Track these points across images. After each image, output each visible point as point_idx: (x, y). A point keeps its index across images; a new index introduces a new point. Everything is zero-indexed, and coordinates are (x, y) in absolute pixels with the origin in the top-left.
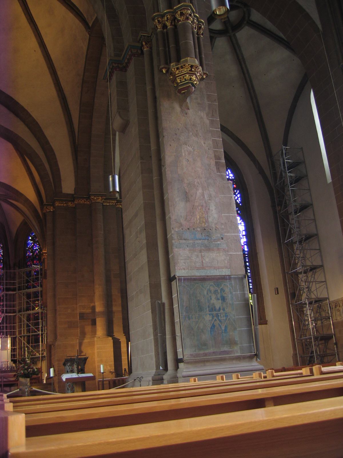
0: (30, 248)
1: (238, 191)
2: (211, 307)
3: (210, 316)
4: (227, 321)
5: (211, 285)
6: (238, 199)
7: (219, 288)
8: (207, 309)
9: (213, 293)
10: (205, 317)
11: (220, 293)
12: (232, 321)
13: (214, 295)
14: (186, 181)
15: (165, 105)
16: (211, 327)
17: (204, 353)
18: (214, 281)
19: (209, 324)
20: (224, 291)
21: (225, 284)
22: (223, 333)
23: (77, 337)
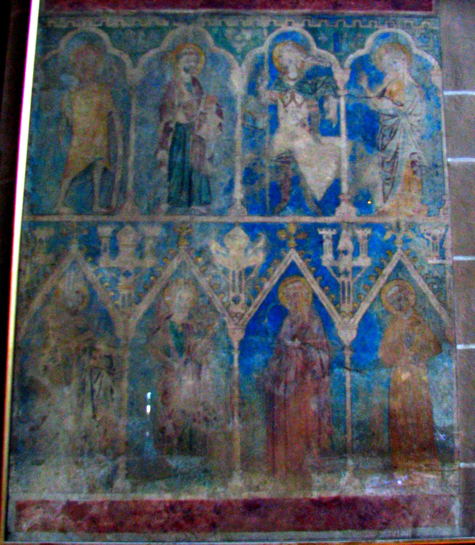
2: (267, 180)
3: (254, 238)
4: (382, 281)
5: (284, 36)
7: (341, 60)
8: (239, 193)
9: (292, 84)
10: (214, 246)
11: (342, 92)
12: (421, 283)
13: (299, 98)
16: (256, 318)
17: (171, 507)
18: (306, 11)
19: (236, 300)
21: (385, 36)
22: (342, 364)
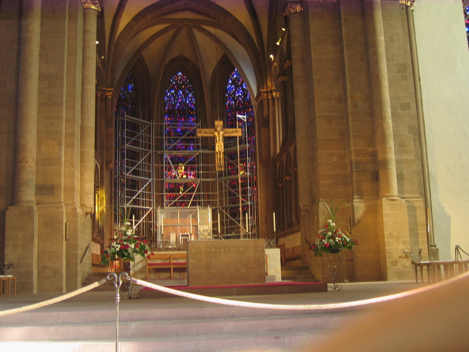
0: (229, 95)
23: (347, 200)
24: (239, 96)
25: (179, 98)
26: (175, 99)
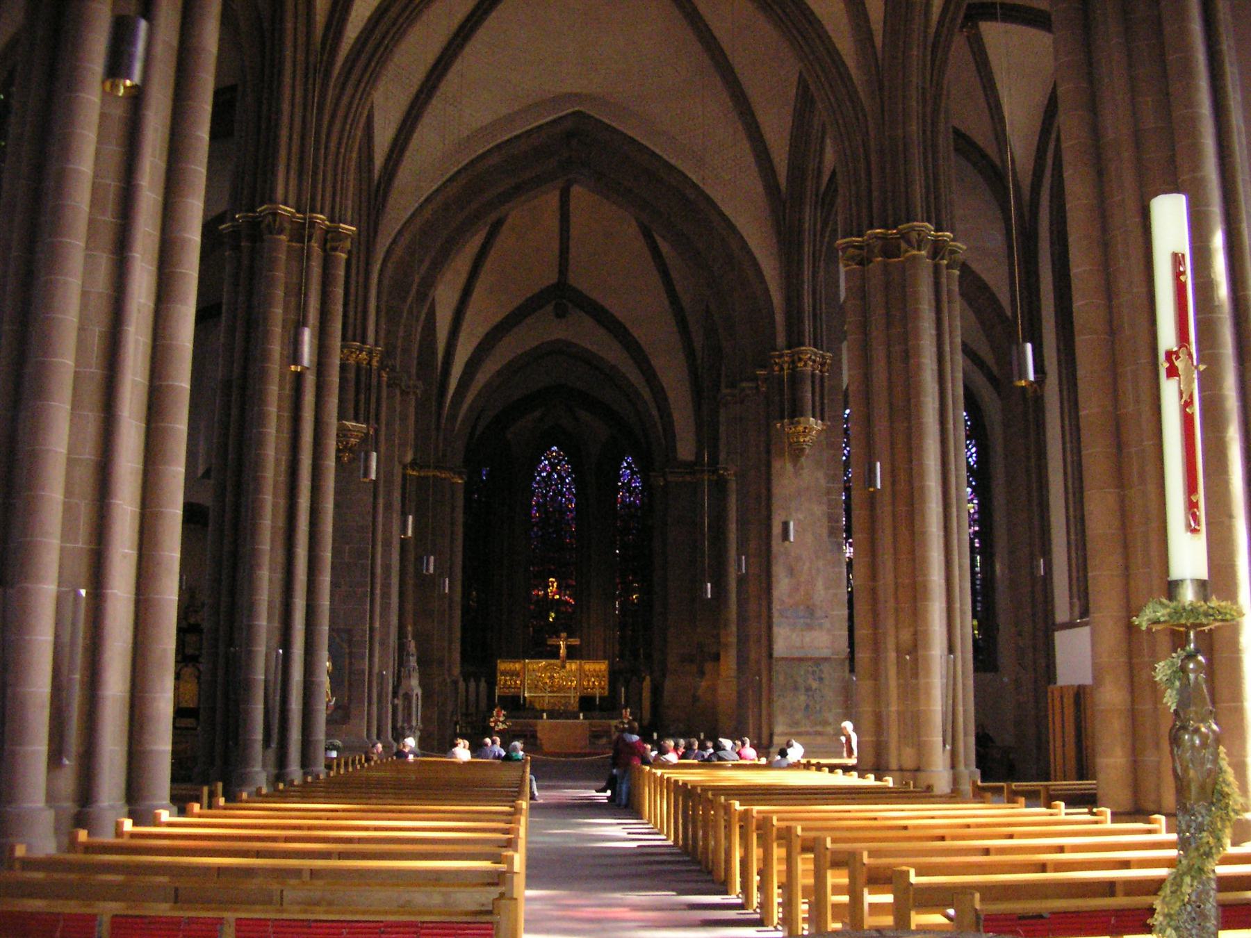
1: (973, 442)
6: (971, 456)
14: (793, 554)
15: (776, 465)
20: (823, 673)
24: (636, 486)
25: (552, 485)
26: (547, 485)
